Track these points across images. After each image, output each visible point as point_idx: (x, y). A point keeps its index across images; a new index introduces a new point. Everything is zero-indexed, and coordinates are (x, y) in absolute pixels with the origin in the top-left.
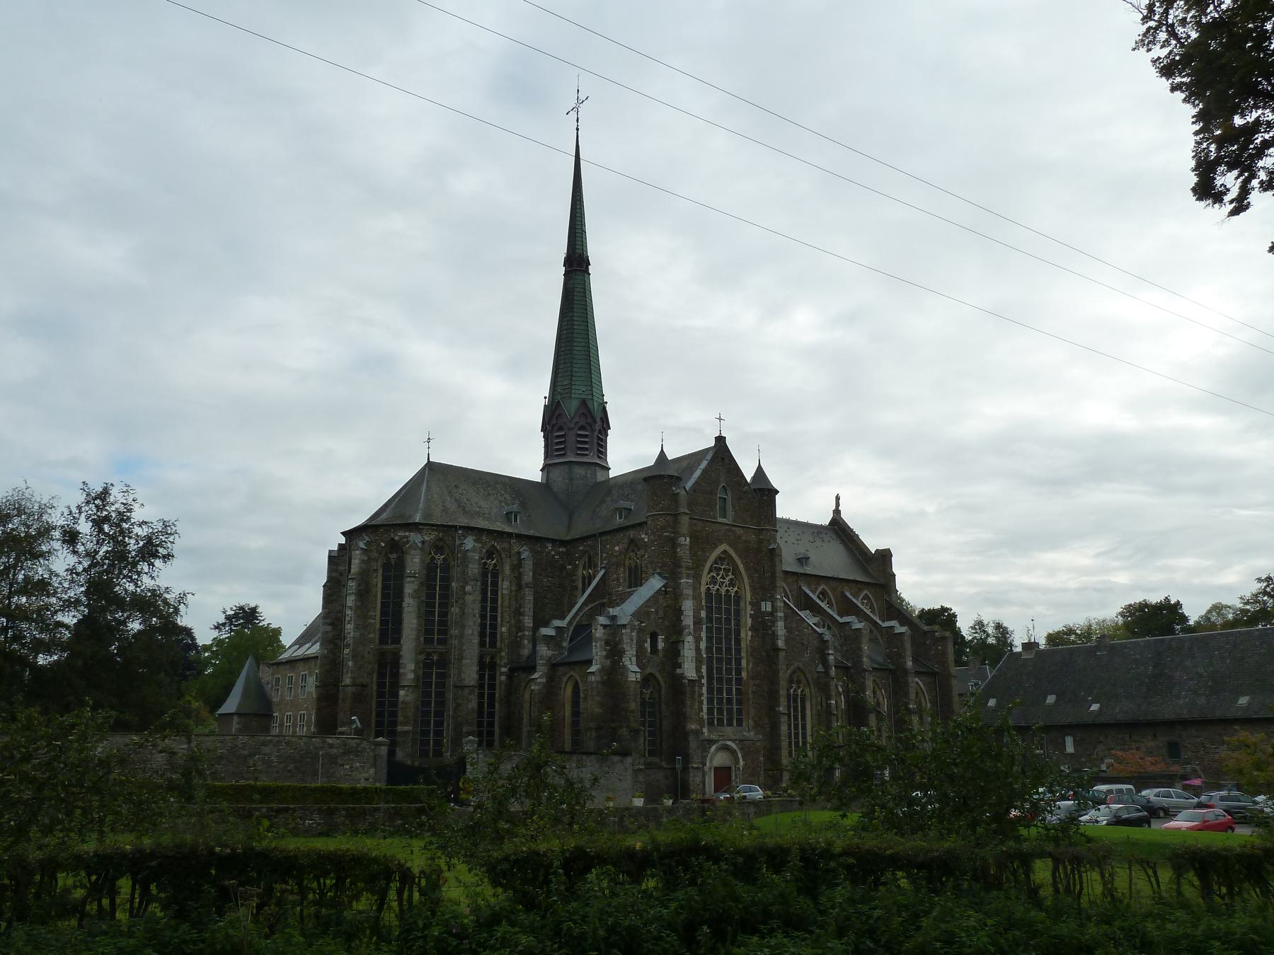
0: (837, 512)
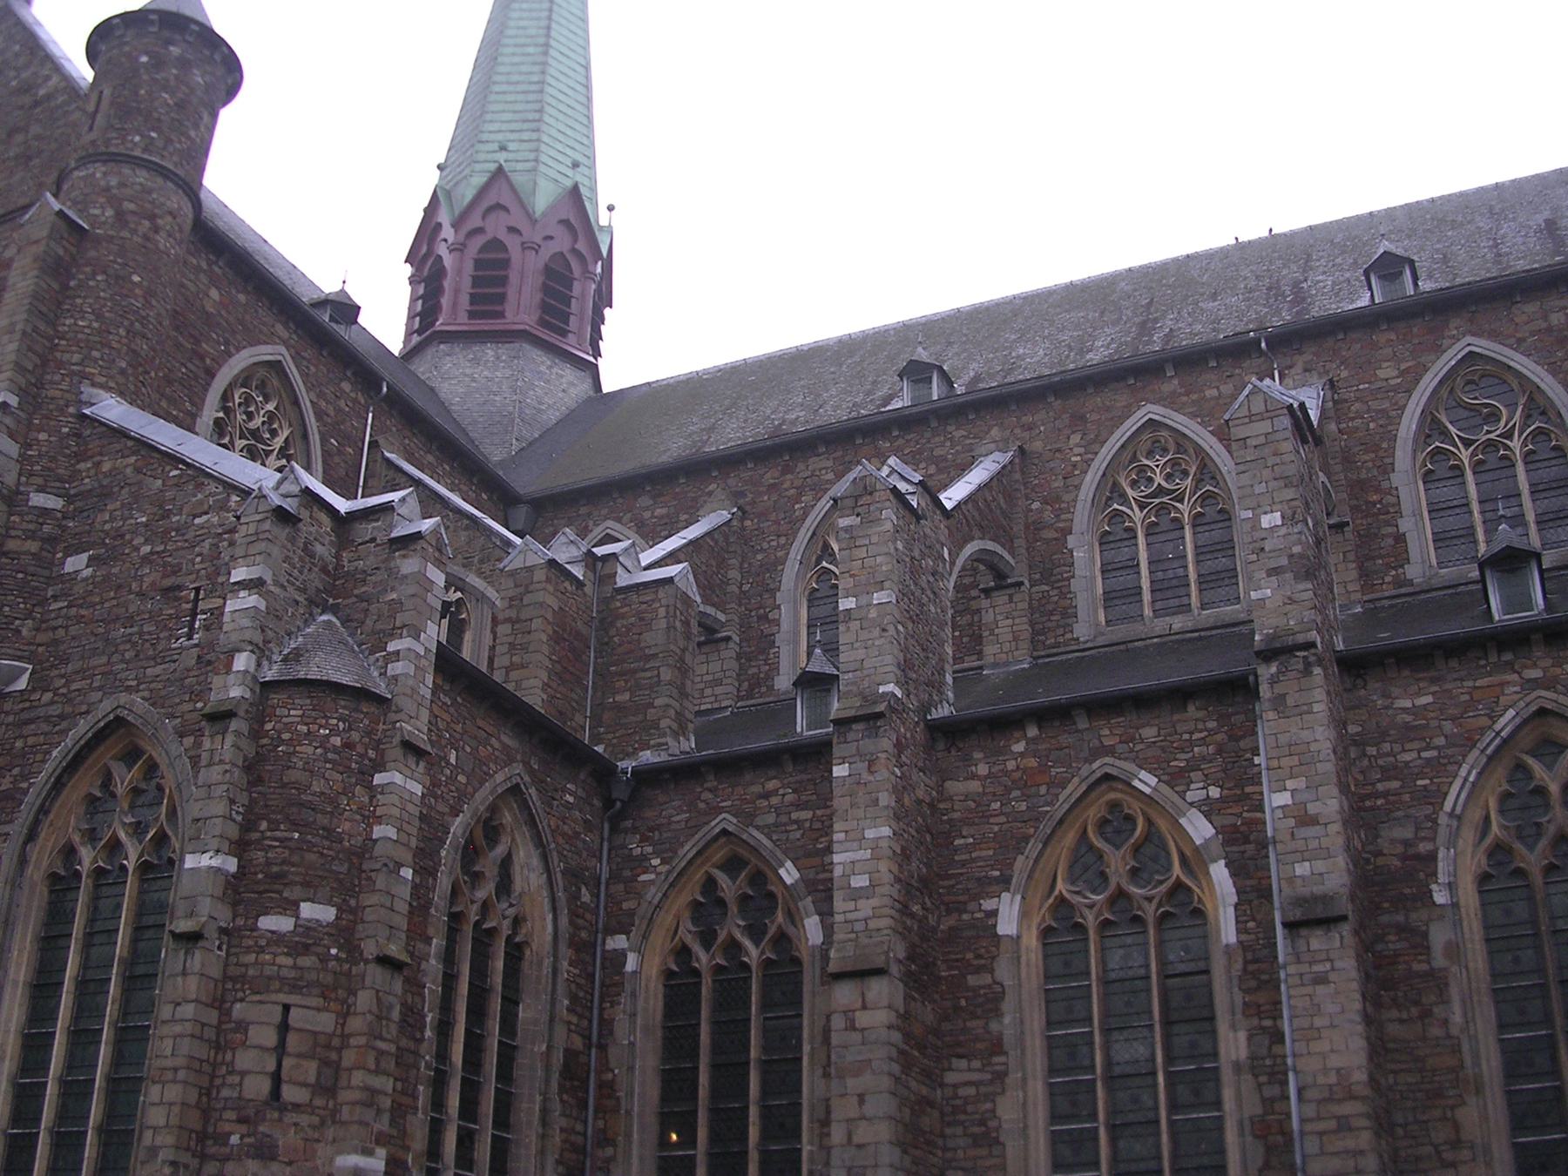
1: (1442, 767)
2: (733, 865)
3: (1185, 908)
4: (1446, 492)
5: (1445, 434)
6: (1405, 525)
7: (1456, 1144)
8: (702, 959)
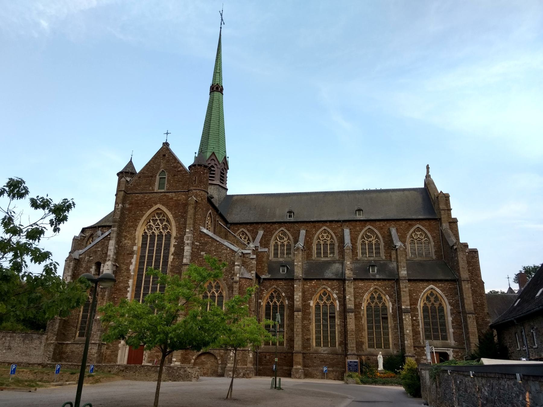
0: (428, 176)
1: (364, 293)
2: (275, 292)
3: (332, 305)
4: (364, 247)
5: (364, 239)
6: (358, 251)
7: (362, 336)
8: (271, 304)
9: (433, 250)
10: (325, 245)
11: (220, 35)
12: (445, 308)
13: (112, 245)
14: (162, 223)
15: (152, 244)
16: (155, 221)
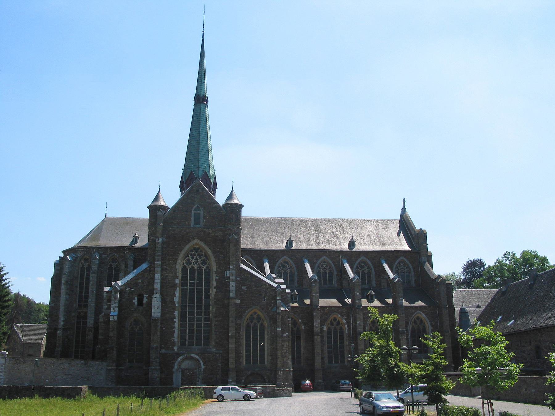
0: (404, 210)
9: (413, 279)
10: (325, 273)
11: (203, 40)
12: (427, 328)
13: (157, 277)
14: (200, 258)
15: (192, 279)
16: (193, 256)
